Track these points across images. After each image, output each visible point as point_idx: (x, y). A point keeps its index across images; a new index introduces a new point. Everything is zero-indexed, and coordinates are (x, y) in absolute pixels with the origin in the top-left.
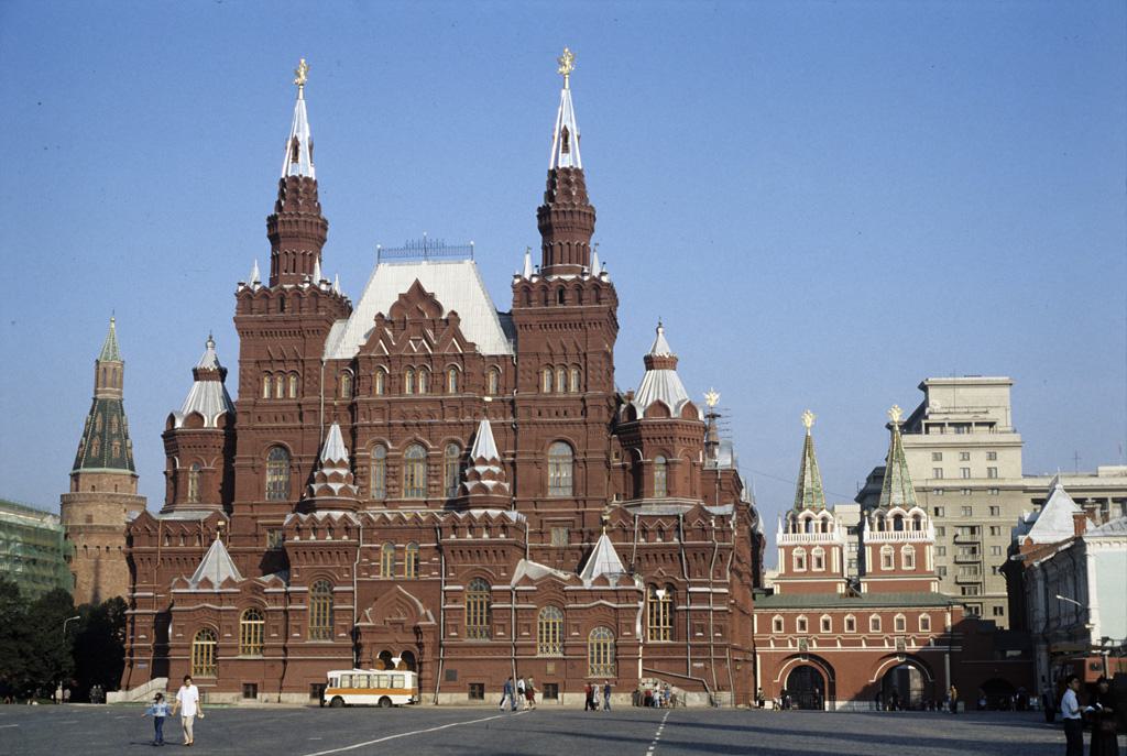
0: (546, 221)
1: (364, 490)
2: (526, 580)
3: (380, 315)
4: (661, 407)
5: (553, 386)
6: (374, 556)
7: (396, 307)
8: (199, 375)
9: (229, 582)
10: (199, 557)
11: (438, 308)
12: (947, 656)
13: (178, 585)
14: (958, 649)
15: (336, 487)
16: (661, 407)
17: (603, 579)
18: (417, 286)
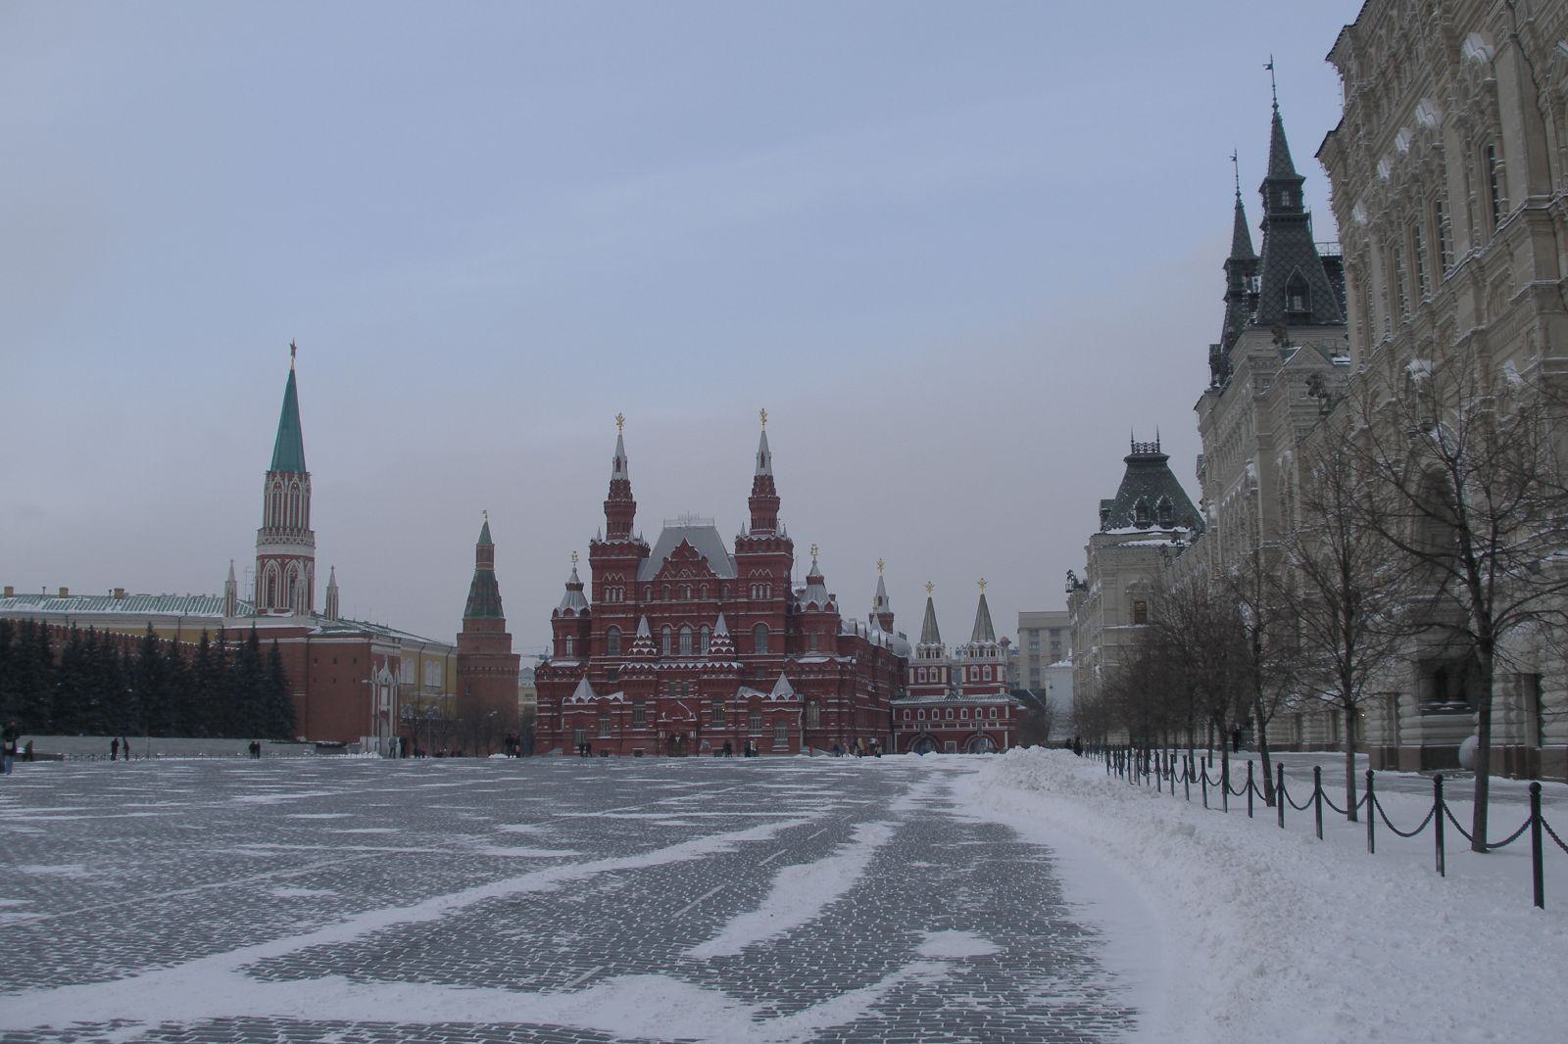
0: (754, 505)
1: (660, 651)
3: (665, 558)
4: (812, 606)
5: (758, 596)
7: (674, 554)
8: (570, 587)
9: (591, 700)
10: (576, 685)
11: (696, 554)
12: (1006, 733)
13: (566, 701)
14: (1012, 728)
15: (646, 650)
16: (812, 606)
17: (780, 697)
18: (685, 543)
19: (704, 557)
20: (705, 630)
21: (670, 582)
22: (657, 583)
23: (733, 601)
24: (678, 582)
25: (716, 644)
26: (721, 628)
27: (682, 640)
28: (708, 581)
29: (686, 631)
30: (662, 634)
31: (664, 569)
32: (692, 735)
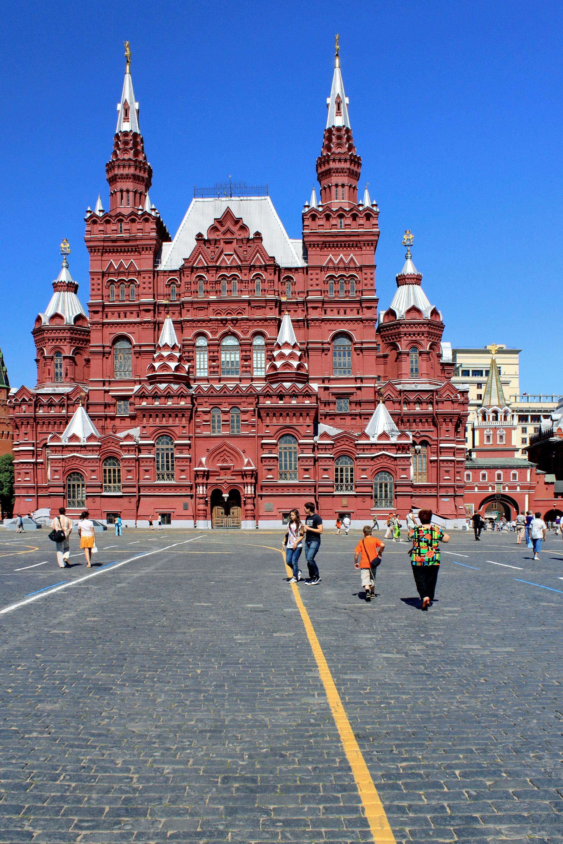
2: (325, 435)
3: (200, 235)
6: (206, 417)
18: (228, 213)
19: (258, 234)
20: (259, 341)
21: (207, 269)
22: (188, 268)
23: (300, 299)
24: (218, 268)
25: (282, 356)
26: (287, 333)
27: (225, 357)
28: (265, 268)
29: (230, 341)
30: (194, 345)
31: (196, 253)
32: (249, 490)
